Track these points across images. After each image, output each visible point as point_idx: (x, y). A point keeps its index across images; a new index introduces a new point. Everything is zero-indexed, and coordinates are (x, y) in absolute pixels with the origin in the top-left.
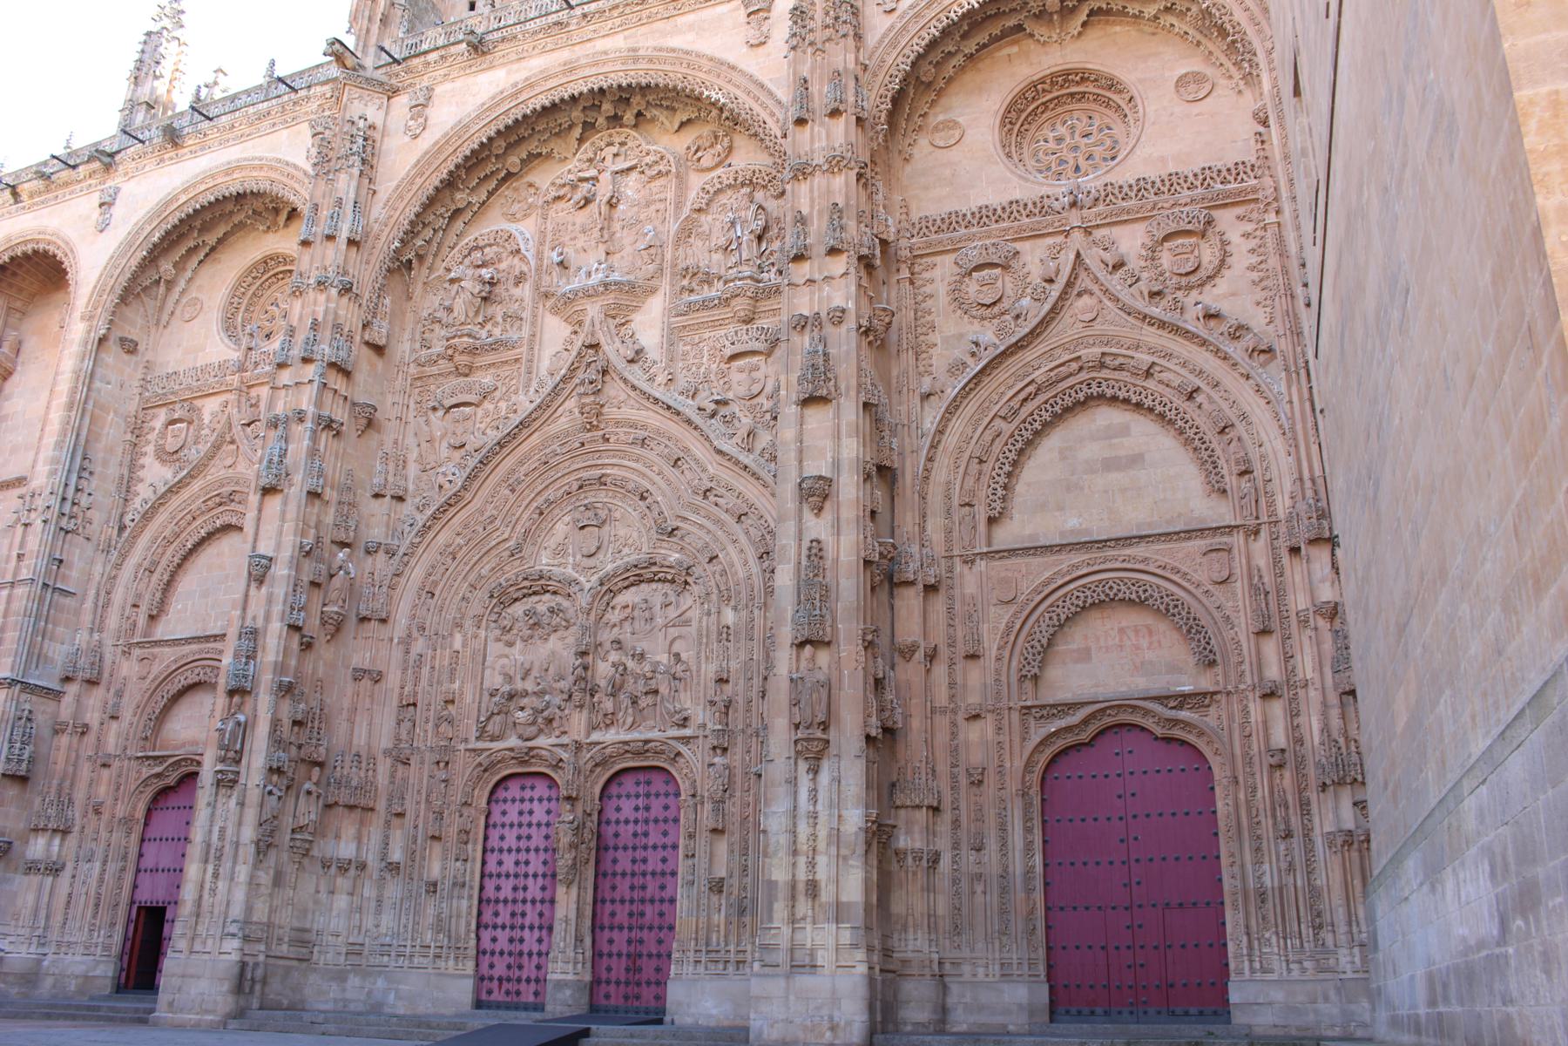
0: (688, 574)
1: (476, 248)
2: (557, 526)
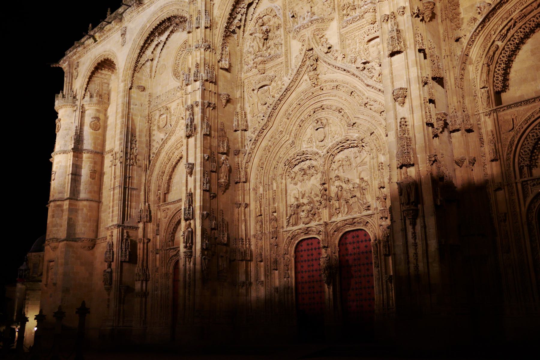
1: (260, 18)
2: (307, 131)
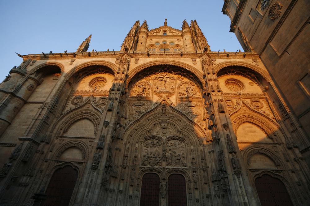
0: (184, 139)
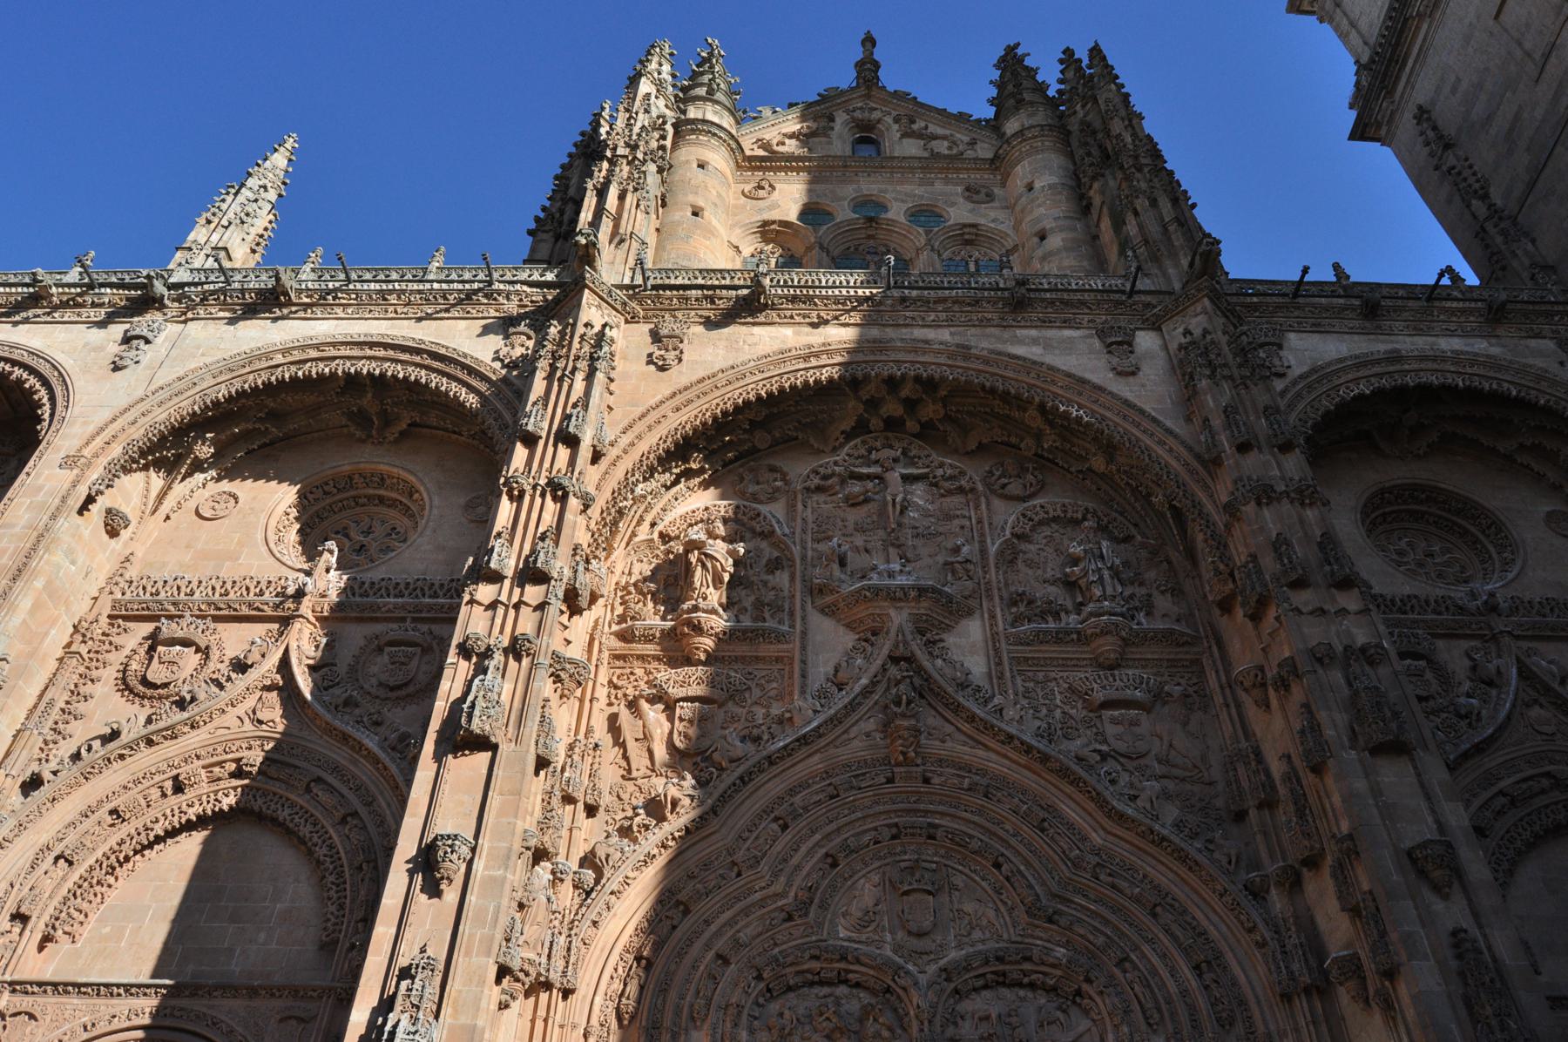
0: (1088, 980)
